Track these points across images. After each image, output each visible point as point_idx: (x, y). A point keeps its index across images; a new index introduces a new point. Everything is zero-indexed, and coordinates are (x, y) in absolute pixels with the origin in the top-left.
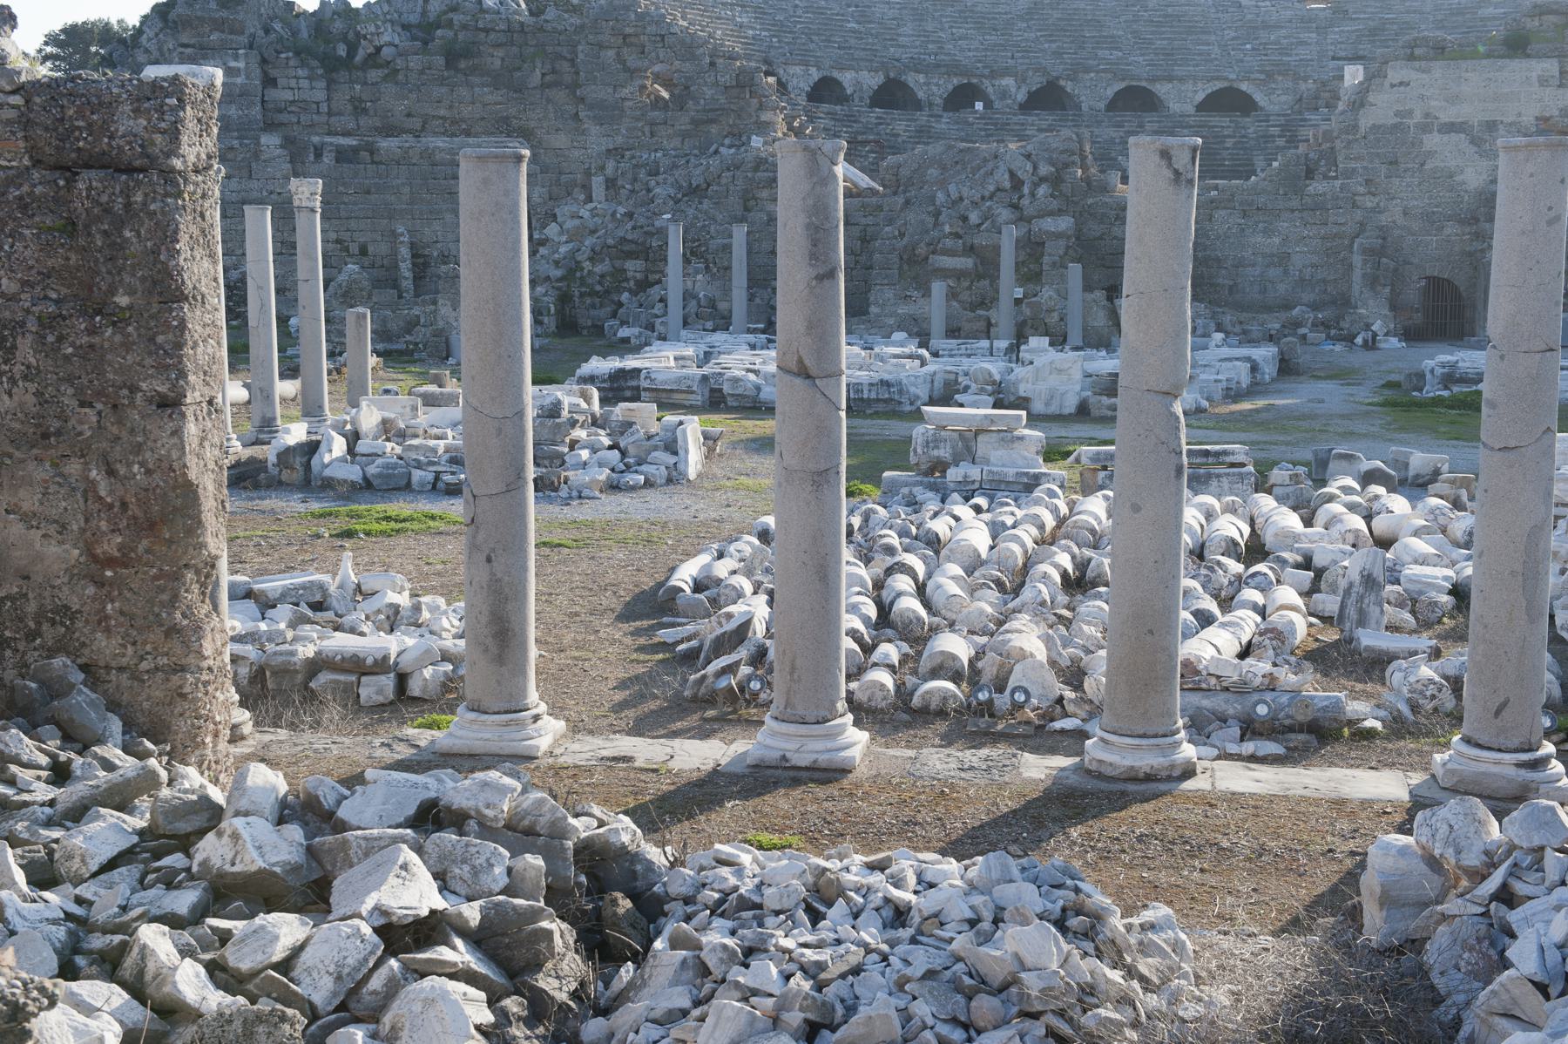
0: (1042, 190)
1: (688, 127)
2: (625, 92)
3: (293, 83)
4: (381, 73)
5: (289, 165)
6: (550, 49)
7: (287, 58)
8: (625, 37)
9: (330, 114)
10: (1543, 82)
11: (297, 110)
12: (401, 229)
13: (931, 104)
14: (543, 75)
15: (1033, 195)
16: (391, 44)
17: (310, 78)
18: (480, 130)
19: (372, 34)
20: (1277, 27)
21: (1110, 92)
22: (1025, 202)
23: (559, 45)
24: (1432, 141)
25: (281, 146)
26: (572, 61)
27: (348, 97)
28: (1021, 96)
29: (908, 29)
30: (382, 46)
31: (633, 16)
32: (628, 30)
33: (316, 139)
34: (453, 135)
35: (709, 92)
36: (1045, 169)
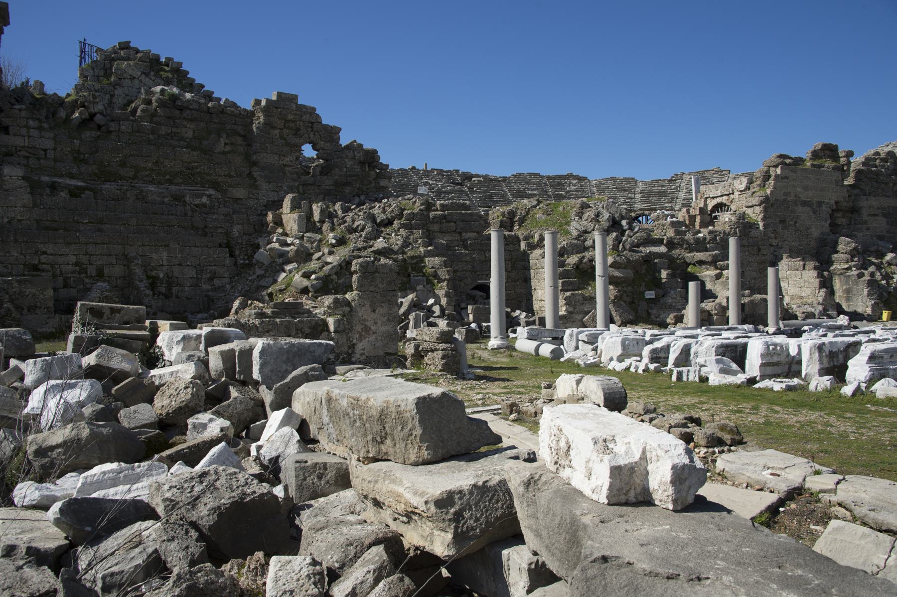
1: (331, 187)
2: (287, 160)
3: (24, 131)
4: (94, 134)
5: (30, 196)
6: (228, 127)
7: (20, 110)
8: (287, 121)
11: (27, 155)
14: (226, 144)
16: (101, 113)
17: (40, 129)
18: (181, 181)
19: (90, 102)
23: (235, 124)
24: (800, 209)
25: (23, 178)
26: (244, 136)
27: (69, 149)
30: (95, 114)
31: (294, 106)
32: (290, 117)
34: (159, 183)
35: (349, 163)
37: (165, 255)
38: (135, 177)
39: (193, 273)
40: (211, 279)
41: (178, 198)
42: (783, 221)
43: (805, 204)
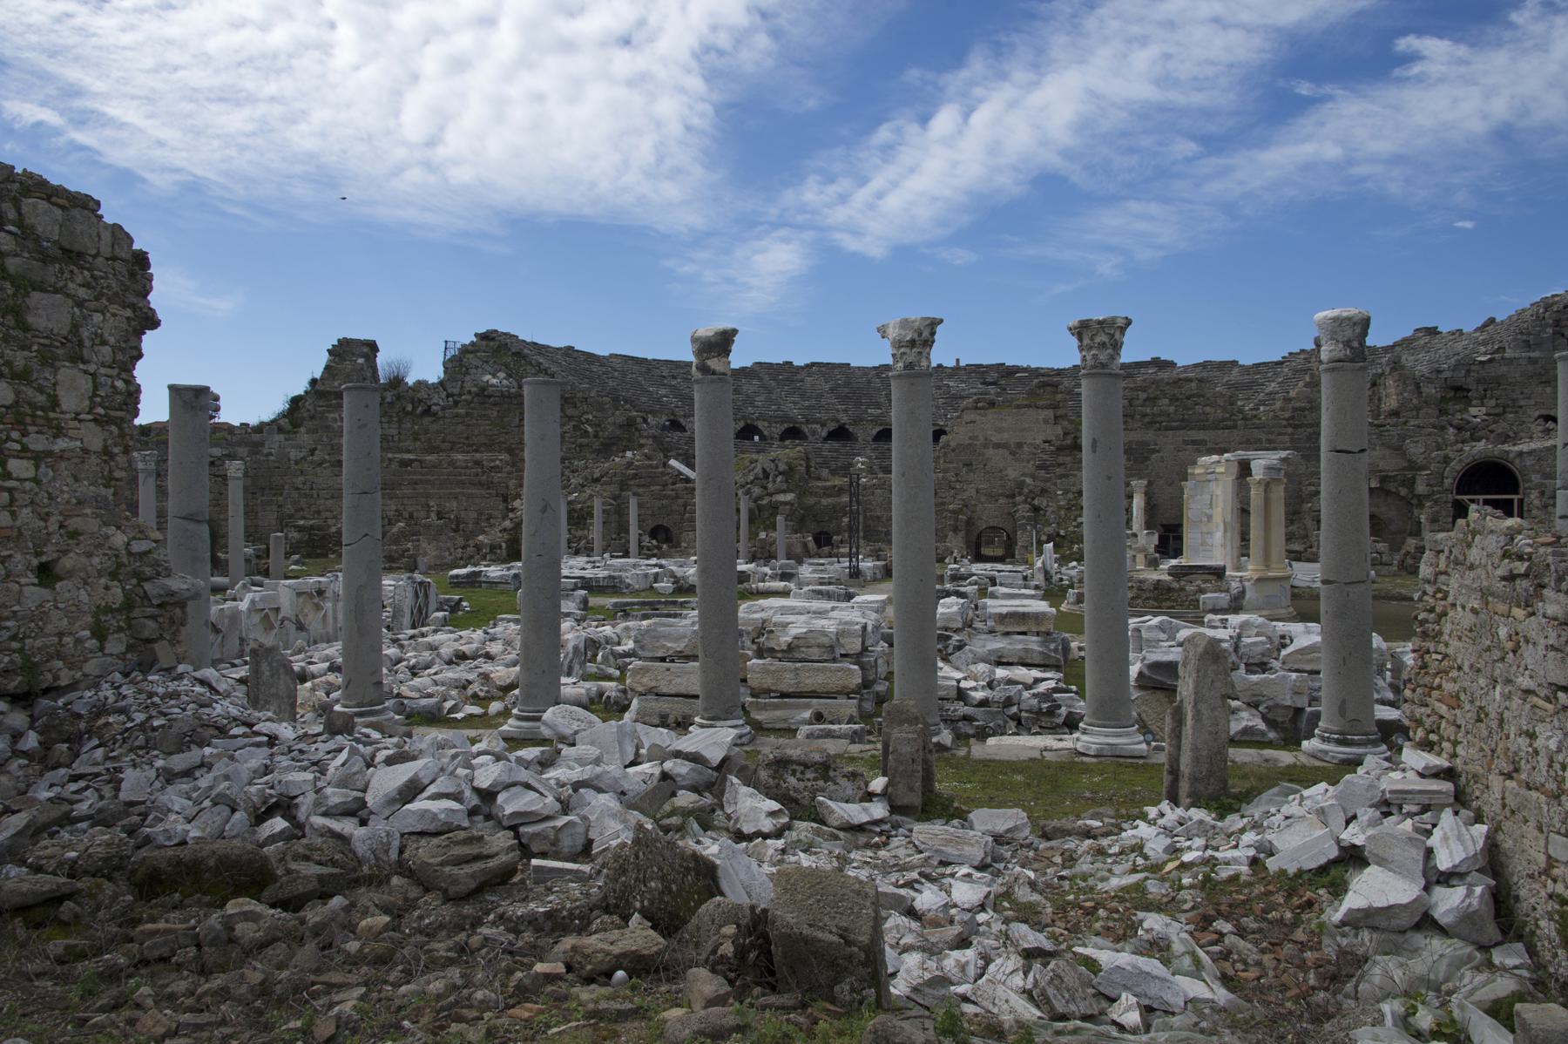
0: (779, 479)
4: (431, 419)
9: (400, 441)
10: (1046, 422)
12: (432, 504)
13: (772, 438)
15: (774, 481)
20: (968, 397)
21: (874, 432)
22: (770, 485)
24: (991, 452)
28: (824, 434)
29: (762, 398)
33: (390, 455)
35: (610, 428)
36: (782, 467)
37: (455, 504)
38: (452, 449)
39: (475, 515)
40: (488, 519)
41: (478, 463)
42: (968, 465)
43: (997, 446)
